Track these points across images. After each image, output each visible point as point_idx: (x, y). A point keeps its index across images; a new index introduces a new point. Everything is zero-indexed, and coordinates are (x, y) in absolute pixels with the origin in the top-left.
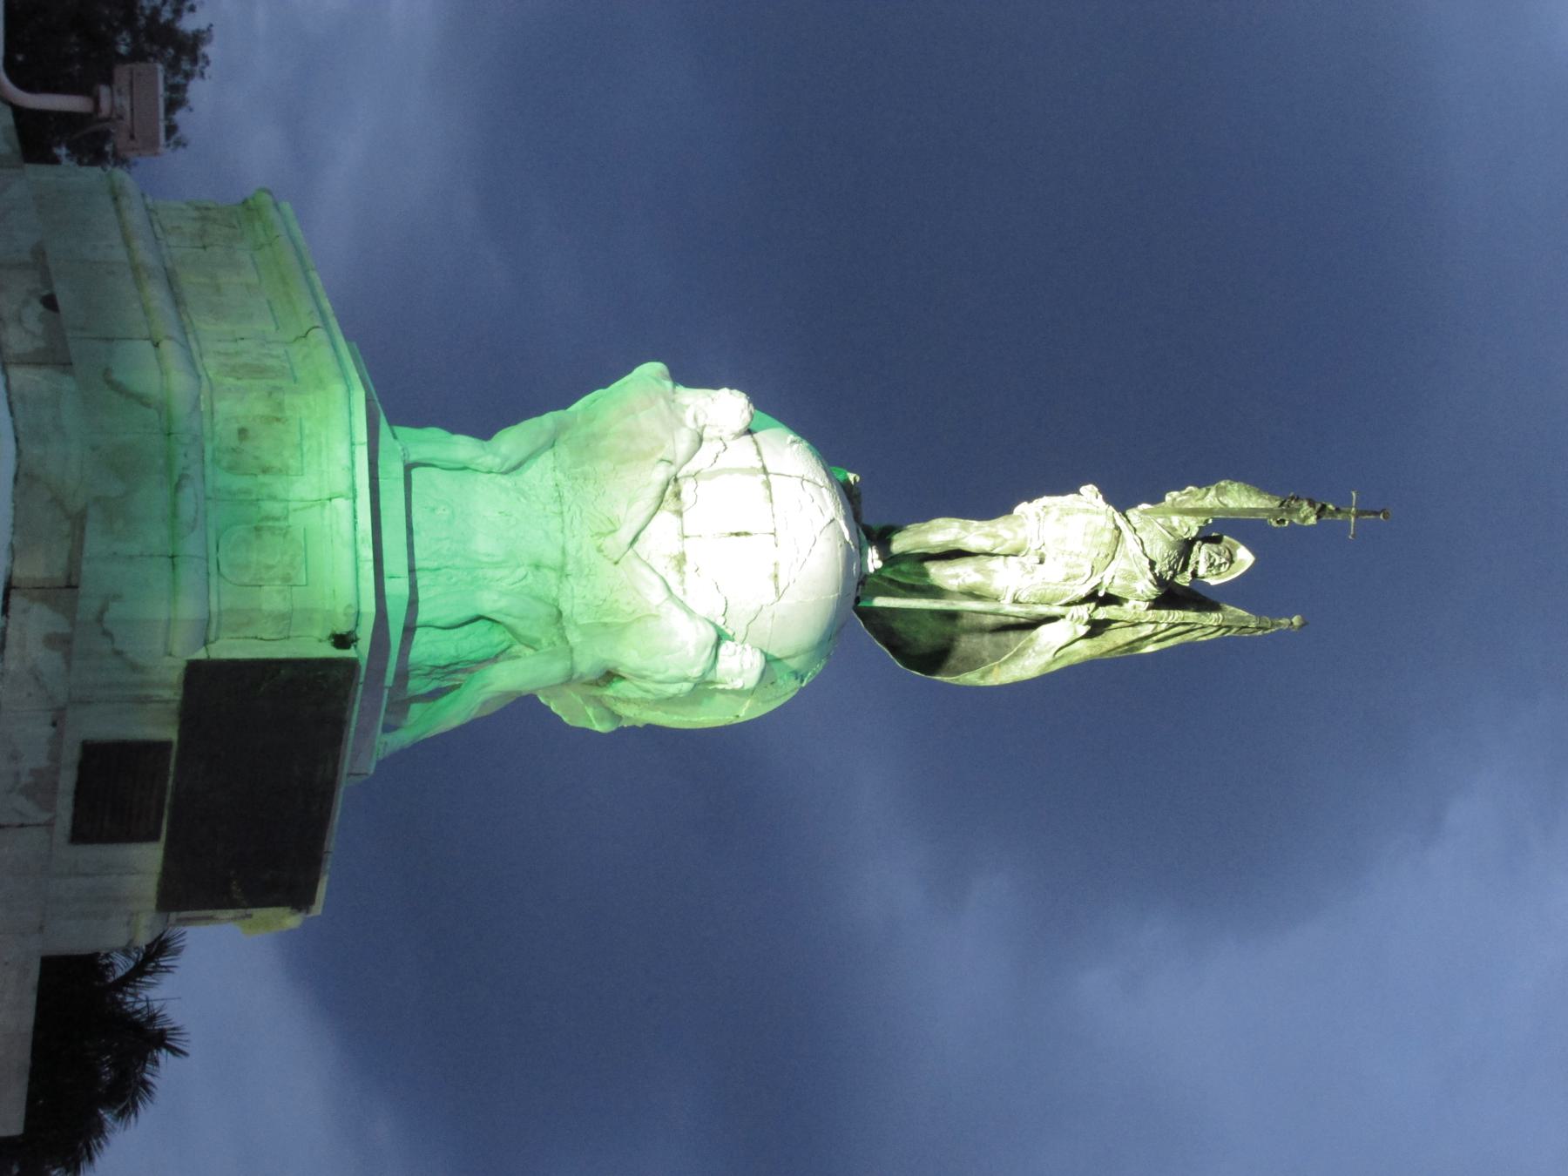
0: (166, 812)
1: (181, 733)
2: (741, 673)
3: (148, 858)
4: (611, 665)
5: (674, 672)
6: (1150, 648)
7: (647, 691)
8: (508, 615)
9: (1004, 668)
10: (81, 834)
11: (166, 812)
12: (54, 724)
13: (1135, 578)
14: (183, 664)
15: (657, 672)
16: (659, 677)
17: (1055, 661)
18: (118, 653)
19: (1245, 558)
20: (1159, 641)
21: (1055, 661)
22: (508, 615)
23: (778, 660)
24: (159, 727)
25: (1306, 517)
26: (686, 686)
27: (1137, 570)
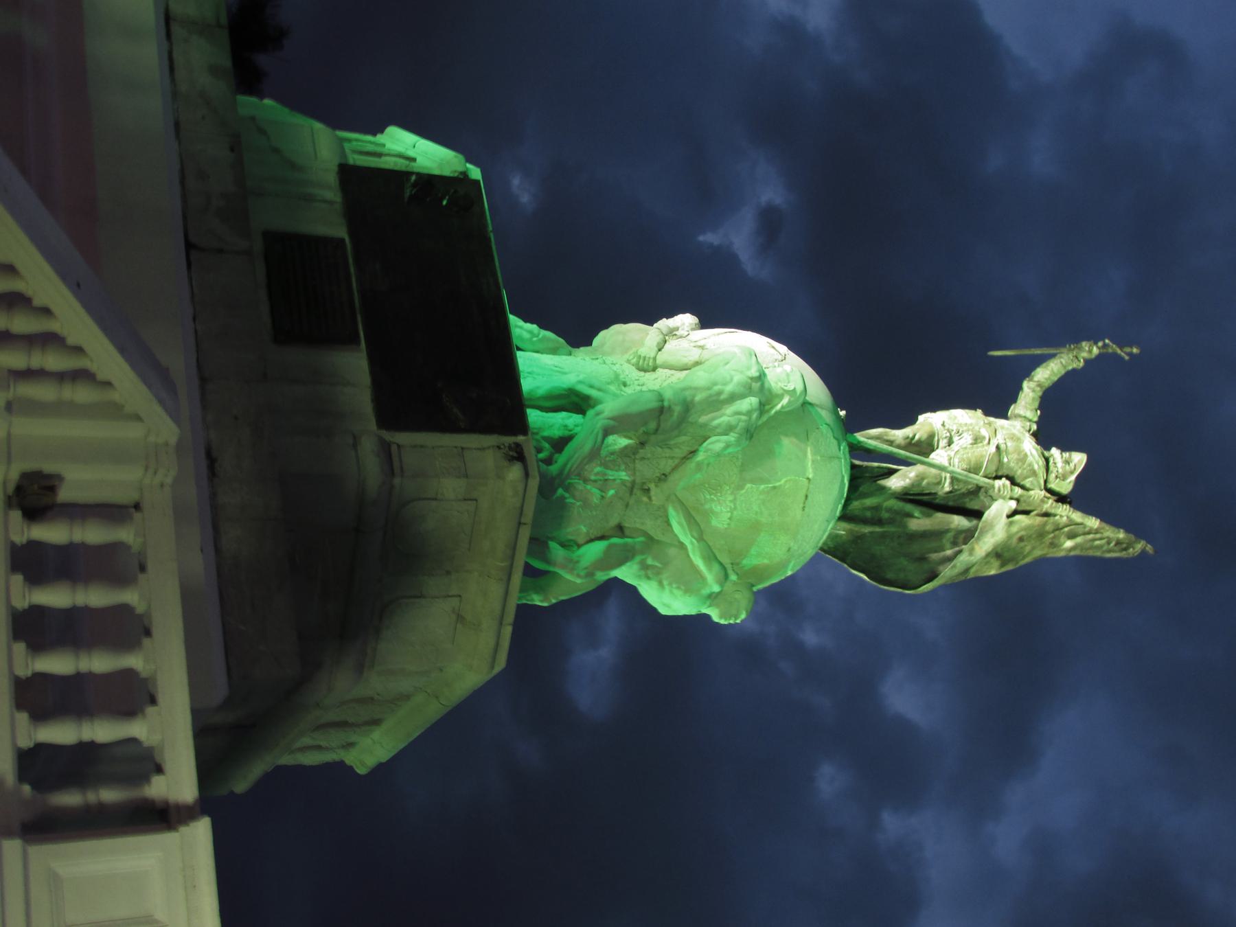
0: (359, 319)
1: (352, 233)
2: (788, 375)
3: (354, 367)
4: (687, 393)
5: (738, 378)
6: (1069, 544)
7: (729, 429)
8: (591, 387)
9: (981, 543)
10: (284, 334)
11: (359, 319)
12: (232, 150)
13: (1018, 440)
14: (335, 169)
15: (725, 384)
16: (729, 388)
17: (1011, 524)
18: (276, 151)
19: (1079, 459)
20: (1071, 536)
21: (1011, 524)
22: (591, 387)
23: (810, 404)
24: (329, 224)
25: (1090, 351)
26: (750, 402)
27: (1015, 432)
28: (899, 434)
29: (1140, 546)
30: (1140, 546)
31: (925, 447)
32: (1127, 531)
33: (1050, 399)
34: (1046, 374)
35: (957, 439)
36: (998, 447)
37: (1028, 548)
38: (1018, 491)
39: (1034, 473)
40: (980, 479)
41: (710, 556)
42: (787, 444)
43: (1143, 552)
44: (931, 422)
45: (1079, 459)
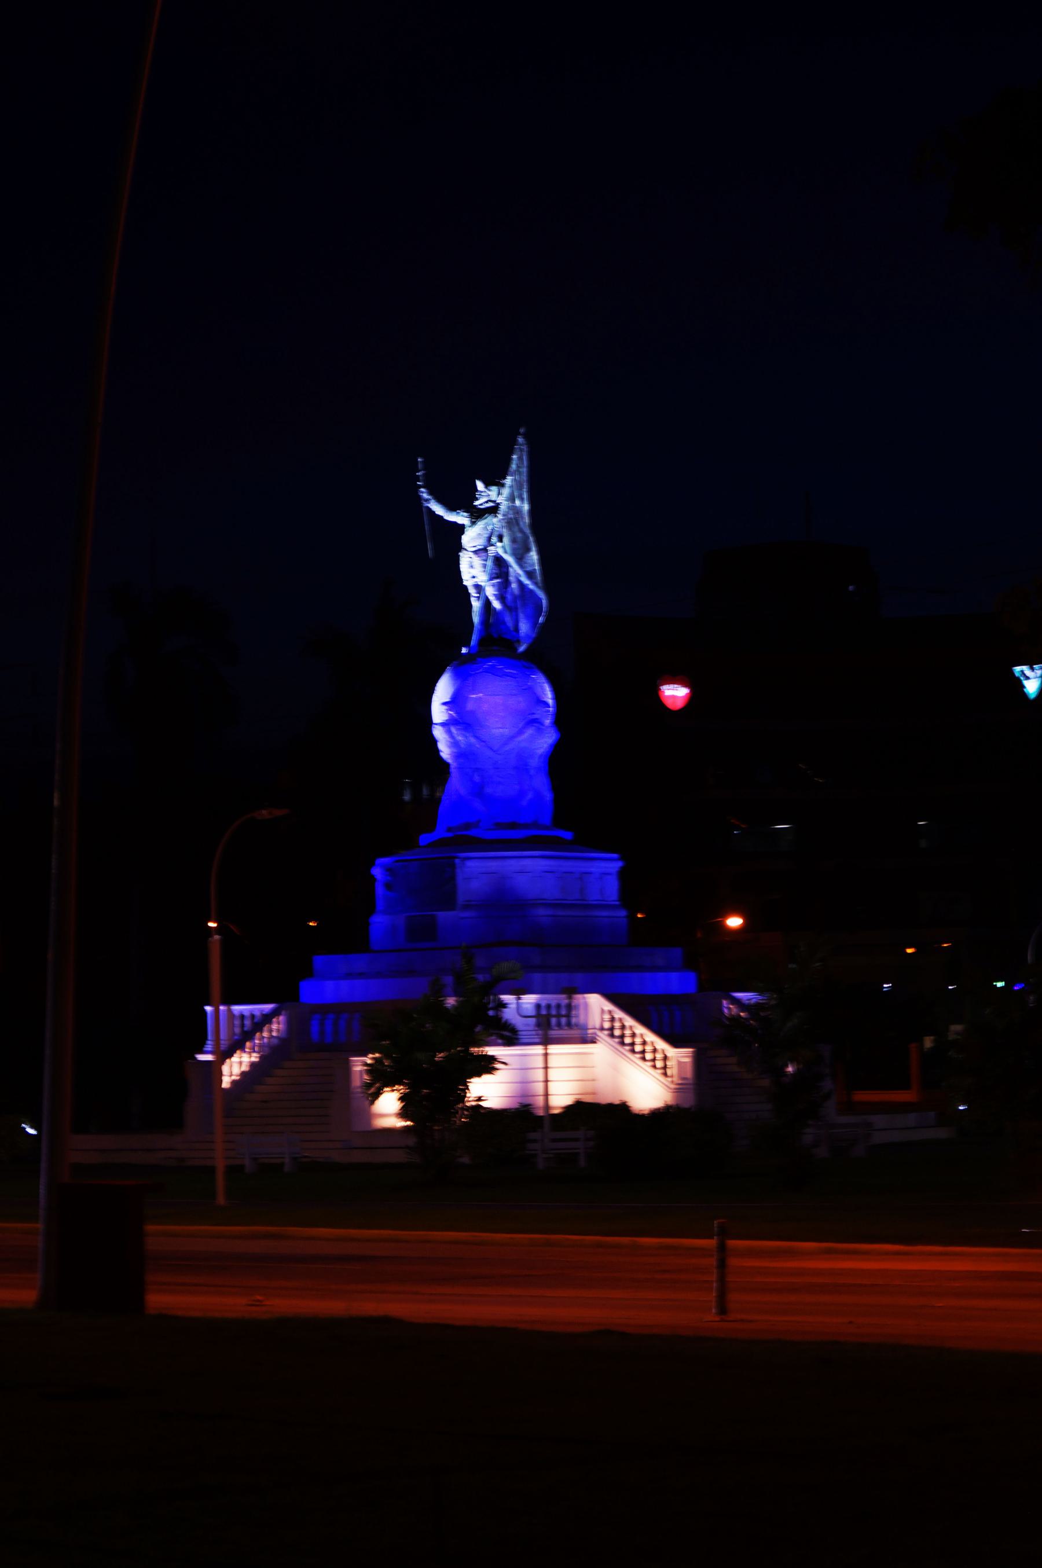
26: (453, 730)
28: (476, 604)
29: (520, 440)
30: (520, 440)
31: (478, 588)
32: (512, 453)
33: (452, 508)
34: (438, 509)
35: (473, 571)
36: (475, 552)
37: (519, 535)
38: (494, 539)
39: (487, 524)
40: (490, 563)
41: (520, 732)
42: (470, 706)
43: (525, 436)
44: (468, 582)
45: (480, 485)
